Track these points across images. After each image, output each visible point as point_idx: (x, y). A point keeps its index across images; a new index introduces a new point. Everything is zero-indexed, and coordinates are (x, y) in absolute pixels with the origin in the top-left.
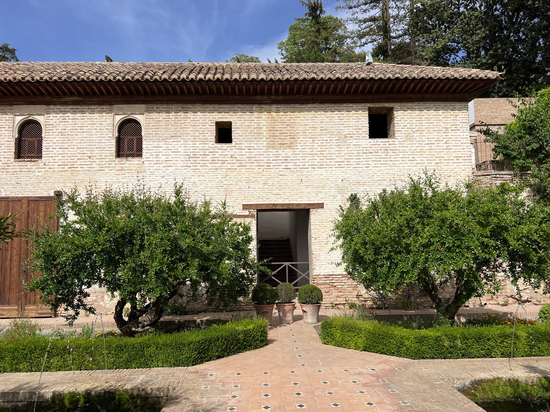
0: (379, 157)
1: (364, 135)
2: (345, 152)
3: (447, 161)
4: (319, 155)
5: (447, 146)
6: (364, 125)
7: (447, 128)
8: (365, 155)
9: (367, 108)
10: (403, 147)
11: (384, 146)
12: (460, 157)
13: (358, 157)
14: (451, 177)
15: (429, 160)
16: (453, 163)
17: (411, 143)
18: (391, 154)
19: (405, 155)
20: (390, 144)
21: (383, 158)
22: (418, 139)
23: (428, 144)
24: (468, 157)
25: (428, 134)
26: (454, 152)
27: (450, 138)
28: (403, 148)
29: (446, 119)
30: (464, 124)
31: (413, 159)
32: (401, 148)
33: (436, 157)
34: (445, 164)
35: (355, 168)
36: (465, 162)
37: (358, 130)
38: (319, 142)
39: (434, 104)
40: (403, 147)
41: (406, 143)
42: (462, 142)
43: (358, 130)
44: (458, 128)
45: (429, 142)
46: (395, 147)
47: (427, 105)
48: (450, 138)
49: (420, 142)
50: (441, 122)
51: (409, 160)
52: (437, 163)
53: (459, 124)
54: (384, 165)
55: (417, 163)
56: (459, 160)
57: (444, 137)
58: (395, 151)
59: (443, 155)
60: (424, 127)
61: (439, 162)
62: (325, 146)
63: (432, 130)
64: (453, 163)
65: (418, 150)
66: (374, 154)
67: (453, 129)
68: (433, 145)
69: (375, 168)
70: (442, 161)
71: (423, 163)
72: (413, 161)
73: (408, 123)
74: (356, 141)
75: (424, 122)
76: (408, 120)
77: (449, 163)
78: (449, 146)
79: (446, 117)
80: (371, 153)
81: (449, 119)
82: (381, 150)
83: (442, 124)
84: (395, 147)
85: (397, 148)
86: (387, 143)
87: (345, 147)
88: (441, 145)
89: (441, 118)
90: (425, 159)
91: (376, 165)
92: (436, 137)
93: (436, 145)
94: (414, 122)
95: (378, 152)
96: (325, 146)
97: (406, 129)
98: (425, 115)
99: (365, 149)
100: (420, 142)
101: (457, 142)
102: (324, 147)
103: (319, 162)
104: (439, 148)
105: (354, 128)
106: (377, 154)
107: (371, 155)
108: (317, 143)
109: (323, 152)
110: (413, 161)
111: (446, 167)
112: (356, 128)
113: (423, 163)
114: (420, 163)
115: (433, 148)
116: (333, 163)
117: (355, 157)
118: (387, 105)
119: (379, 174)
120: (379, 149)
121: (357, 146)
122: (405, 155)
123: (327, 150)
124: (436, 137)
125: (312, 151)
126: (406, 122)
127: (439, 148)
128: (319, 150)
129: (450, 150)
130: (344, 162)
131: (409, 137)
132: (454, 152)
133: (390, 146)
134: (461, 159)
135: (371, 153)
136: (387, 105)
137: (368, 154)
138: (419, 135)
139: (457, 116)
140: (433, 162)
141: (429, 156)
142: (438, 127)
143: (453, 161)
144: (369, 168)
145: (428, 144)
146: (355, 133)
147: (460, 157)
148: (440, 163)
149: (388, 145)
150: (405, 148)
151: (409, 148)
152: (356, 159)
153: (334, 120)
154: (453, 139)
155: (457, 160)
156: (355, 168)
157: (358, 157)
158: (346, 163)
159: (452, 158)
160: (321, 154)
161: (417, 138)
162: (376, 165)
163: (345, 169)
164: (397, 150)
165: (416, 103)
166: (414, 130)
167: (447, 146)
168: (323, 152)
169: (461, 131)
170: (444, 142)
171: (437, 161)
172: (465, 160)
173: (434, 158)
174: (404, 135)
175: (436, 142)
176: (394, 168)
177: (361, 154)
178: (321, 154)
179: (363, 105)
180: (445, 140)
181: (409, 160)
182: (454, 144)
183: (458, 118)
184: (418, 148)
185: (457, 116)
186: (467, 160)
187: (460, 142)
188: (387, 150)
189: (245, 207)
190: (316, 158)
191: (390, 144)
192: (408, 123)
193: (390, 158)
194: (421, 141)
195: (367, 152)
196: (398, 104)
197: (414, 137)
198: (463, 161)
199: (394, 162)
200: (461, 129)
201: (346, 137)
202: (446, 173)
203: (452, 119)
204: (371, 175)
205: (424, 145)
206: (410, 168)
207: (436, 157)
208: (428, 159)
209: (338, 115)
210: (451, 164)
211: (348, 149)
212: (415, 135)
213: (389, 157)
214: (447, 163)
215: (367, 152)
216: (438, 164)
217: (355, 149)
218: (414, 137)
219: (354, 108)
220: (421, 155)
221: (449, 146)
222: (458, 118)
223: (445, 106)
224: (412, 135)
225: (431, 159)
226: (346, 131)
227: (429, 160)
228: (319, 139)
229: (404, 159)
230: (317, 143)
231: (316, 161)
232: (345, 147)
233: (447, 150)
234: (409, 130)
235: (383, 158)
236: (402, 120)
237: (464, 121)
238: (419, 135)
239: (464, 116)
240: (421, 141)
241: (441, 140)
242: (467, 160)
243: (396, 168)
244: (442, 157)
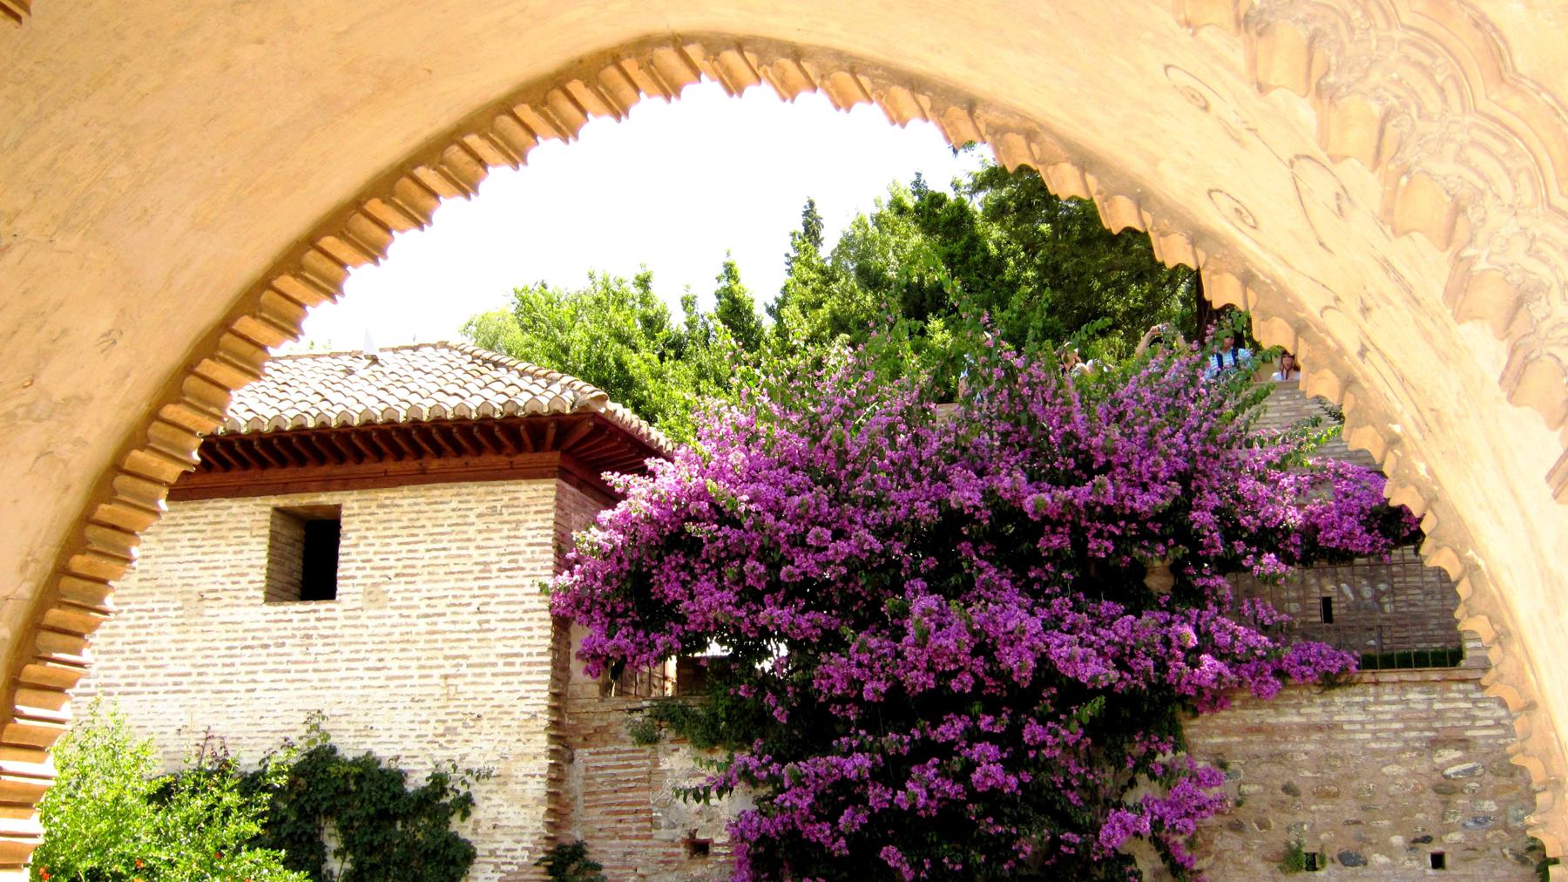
0: (285, 659)
1: (251, 593)
2: (196, 645)
3: (478, 670)
4: (127, 655)
5: (480, 623)
6: (254, 562)
7: (485, 563)
8: (249, 652)
9: (269, 509)
10: (355, 626)
11: (302, 625)
12: (516, 655)
13: (228, 661)
14: (484, 722)
15: (424, 667)
16: (494, 675)
17: (379, 613)
18: (319, 649)
19: (358, 652)
20: (318, 619)
21: (296, 662)
22: (398, 603)
23: (427, 616)
24: (539, 654)
25: (430, 586)
26: (500, 639)
27: (493, 596)
28: (354, 631)
29: (486, 535)
30: (537, 549)
31: (380, 665)
32: (348, 631)
33: (446, 658)
34: (470, 679)
35: (219, 692)
36: (529, 673)
37: (236, 579)
38: (132, 616)
39: (455, 491)
40: (355, 626)
41: (364, 614)
42: (527, 606)
43: (236, 579)
44: (521, 564)
45: (431, 611)
46: (332, 628)
47: (436, 492)
48: (493, 596)
49: (405, 612)
50: (472, 545)
51: (368, 669)
52: (446, 677)
53: (523, 548)
54: (297, 685)
55: (388, 678)
56: (512, 664)
57: (477, 592)
58: (330, 640)
59: (466, 651)
60: (419, 563)
61: (453, 671)
62: (144, 626)
63: (441, 570)
64: (494, 675)
65: (396, 637)
66: (273, 650)
67: (505, 565)
68: (442, 619)
69: (271, 694)
70: (463, 670)
71: (405, 677)
72: (378, 669)
73: (376, 553)
74: (229, 610)
75: (422, 547)
76: (377, 542)
77: (481, 675)
78: (488, 621)
79: (489, 530)
80: (266, 646)
81: (495, 535)
82: (294, 636)
83: (472, 551)
84: (332, 628)
85: (337, 631)
86: (312, 616)
87: (199, 628)
88: (466, 617)
89: (471, 532)
90: (415, 664)
91: (275, 685)
92: (451, 593)
93: (449, 618)
94: (395, 547)
95: (283, 644)
96: (144, 626)
97: (368, 572)
98: (429, 524)
99: (250, 635)
100: (405, 612)
101: (512, 608)
102: (143, 631)
103: (124, 676)
104: (458, 627)
105: (228, 571)
106: (281, 650)
107: (265, 652)
108: (127, 619)
109: (137, 647)
110: (378, 669)
111: (473, 688)
112: (234, 571)
113: (405, 677)
114: (399, 677)
115: (440, 627)
116: (161, 679)
117: (220, 661)
118: (325, 499)
119: (279, 709)
120: (289, 633)
121: (230, 627)
122: (358, 652)
123: (149, 638)
124: (451, 593)
125: (112, 643)
126: (371, 549)
127: (458, 627)
128: (129, 638)
129: (488, 635)
130: (189, 674)
131: (373, 594)
132: (500, 639)
133: (319, 624)
134: (518, 660)
135: (266, 646)
136: (325, 499)
137: (256, 651)
138: (402, 587)
139: (518, 522)
140: (437, 673)
141: (424, 655)
142: (463, 560)
143: (495, 670)
144: (253, 695)
145: (427, 616)
146: (229, 586)
147: (516, 655)
148: (455, 676)
149: (313, 623)
150: (360, 631)
151: (370, 631)
152: (224, 665)
153: (178, 551)
154: (502, 599)
155: (506, 664)
156: (219, 692)
157: (228, 661)
158: (194, 678)
159: (493, 659)
160: (134, 651)
161: (398, 597)
162: (275, 685)
163: (190, 695)
164: (335, 636)
165: (406, 490)
166: (391, 573)
167: (480, 623)
168: (137, 647)
169: (527, 572)
170: (473, 608)
172: (530, 664)
173: (441, 661)
174: (361, 589)
175: (449, 611)
176: (323, 692)
177: (237, 652)
178: (134, 651)
179: (258, 500)
180: (476, 602)
181: (368, 669)
182: (502, 616)
183: (522, 532)
184: (397, 630)
185: (518, 522)
186: (535, 664)
187: (520, 608)
188: (309, 637)
190: (117, 663)
191: (318, 619)
192: (376, 553)
193: (316, 661)
194: (407, 607)
195: (255, 643)
196: (355, 495)
197: (390, 595)
198: (526, 669)
199: (323, 675)
200: (529, 566)
201: (202, 599)
202: (467, 710)
203: (505, 533)
204: (257, 716)
205: (414, 620)
206: (366, 691)
207: (446, 658)
208: (423, 662)
209: (189, 535)
210: (489, 678)
211: (205, 636)
212: (393, 588)
213: (311, 658)
214: (475, 675)
215: (255, 643)
216: (450, 681)
217: (226, 636)
218: (390, 595)
219: (234, 510)
220: (403, 650)
221: (488, 621)
222: (522, 532)
223: (488, 493)
224: (384, 588)
225: (429, 663)
226: (205, 582)
227: (424, 667)
228: (132, 606)
229: (352, 665)
230: (127, 619)
231: (116, 673)
232: (199, 628)
233: (481, 635)
234: (377, 573)
235: (296, 662)
236: (362, 542)
237: (539, 540)
238: (402, 587)
239: (540, 524)
240: (407, 607)
241: (464, 601)
242: (535, 664)
243: (330, 692)
244: (464, 657)
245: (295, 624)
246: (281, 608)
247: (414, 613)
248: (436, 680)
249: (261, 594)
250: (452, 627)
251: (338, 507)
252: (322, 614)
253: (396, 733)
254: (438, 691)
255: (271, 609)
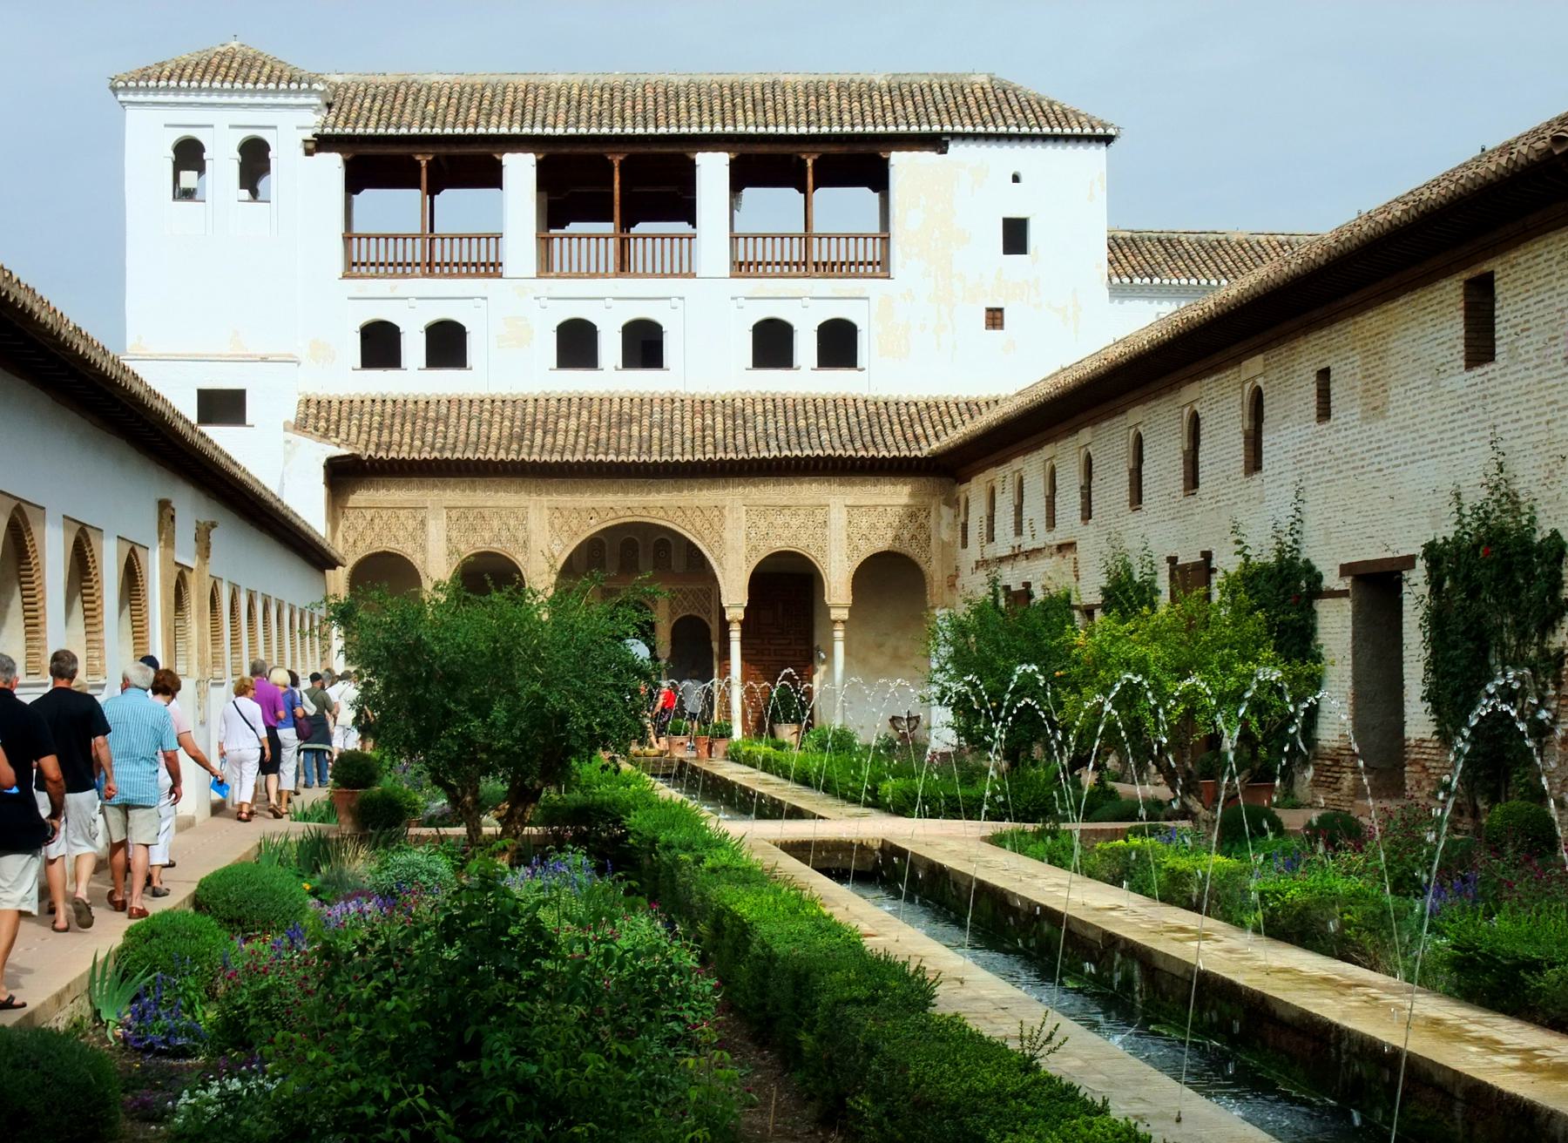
86: (1485, 378)
90: (1532, 413)
118: (1486, 268)
171: (1549, 417)
189: (1346, 570)
216: (1551, 426)
244: (1555, 402)
245: (1480, 387)
246: (1472, 373)
247: (1530, 365)
248: (1543, 427)
249: (1463, 363)
250: (1549, 375)
251: (1492, 273)
252: (1491, 375)
253: (1527, 478)
254: (1544, 436)
255: (1468, 375)
